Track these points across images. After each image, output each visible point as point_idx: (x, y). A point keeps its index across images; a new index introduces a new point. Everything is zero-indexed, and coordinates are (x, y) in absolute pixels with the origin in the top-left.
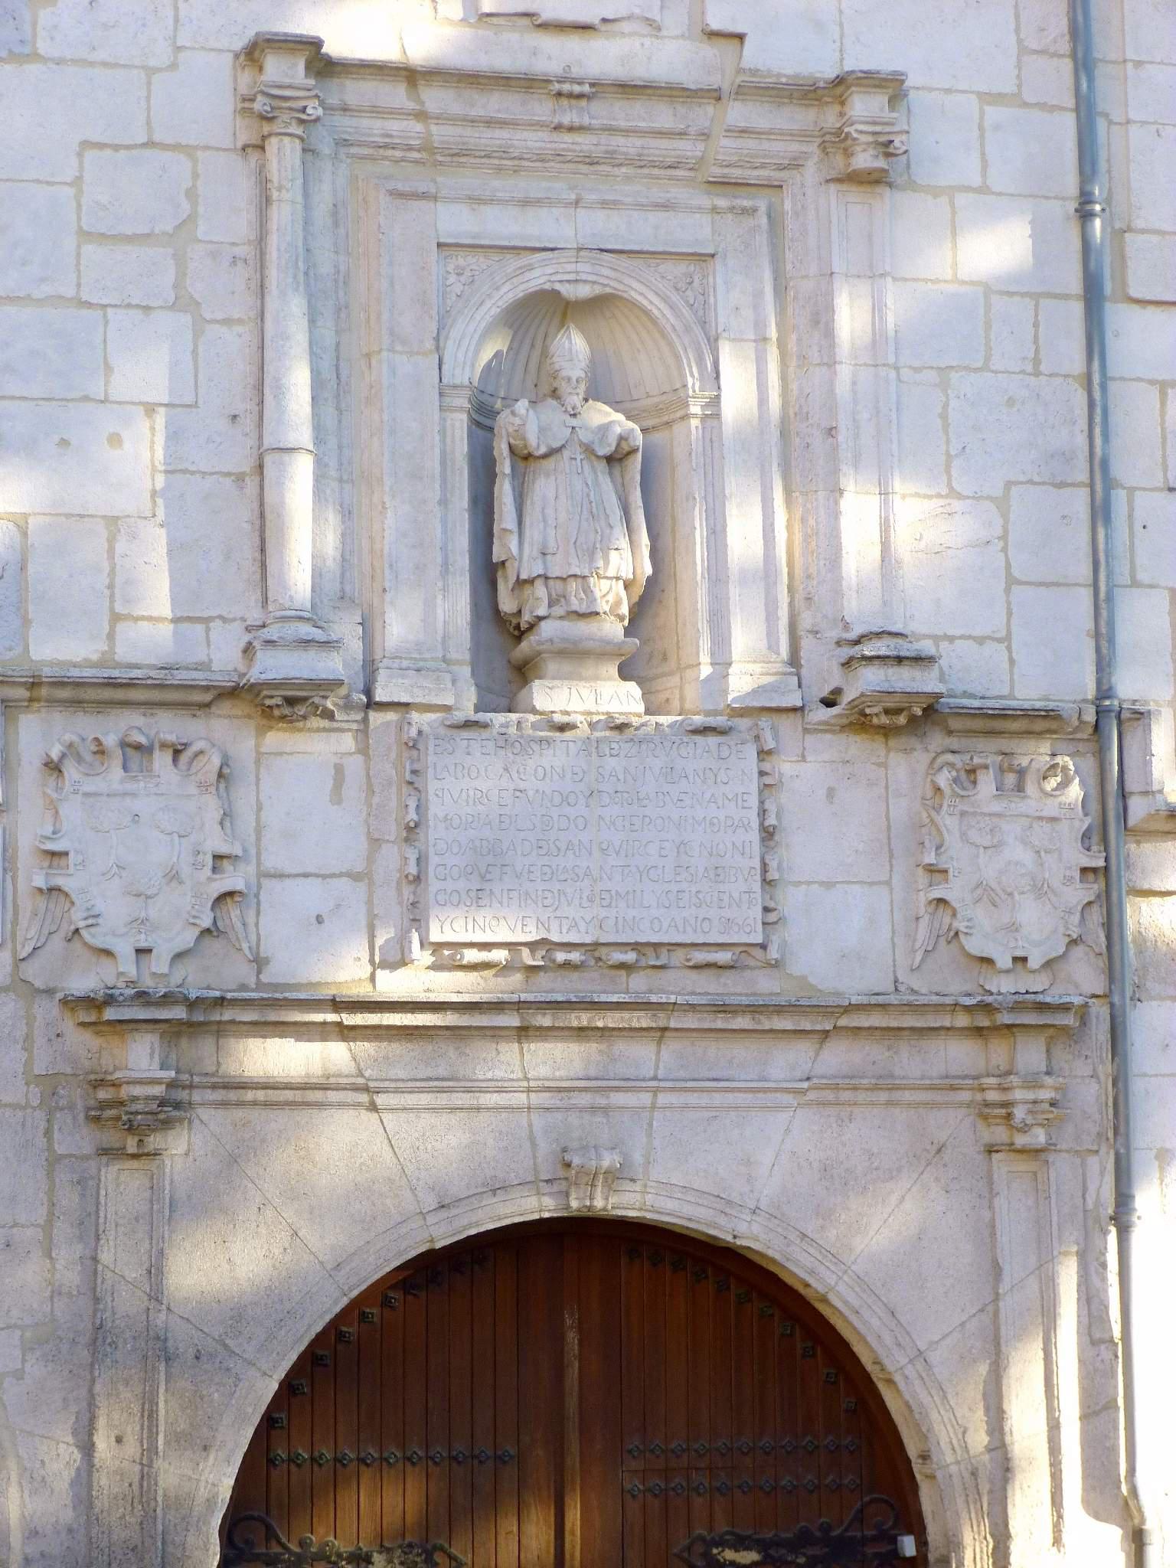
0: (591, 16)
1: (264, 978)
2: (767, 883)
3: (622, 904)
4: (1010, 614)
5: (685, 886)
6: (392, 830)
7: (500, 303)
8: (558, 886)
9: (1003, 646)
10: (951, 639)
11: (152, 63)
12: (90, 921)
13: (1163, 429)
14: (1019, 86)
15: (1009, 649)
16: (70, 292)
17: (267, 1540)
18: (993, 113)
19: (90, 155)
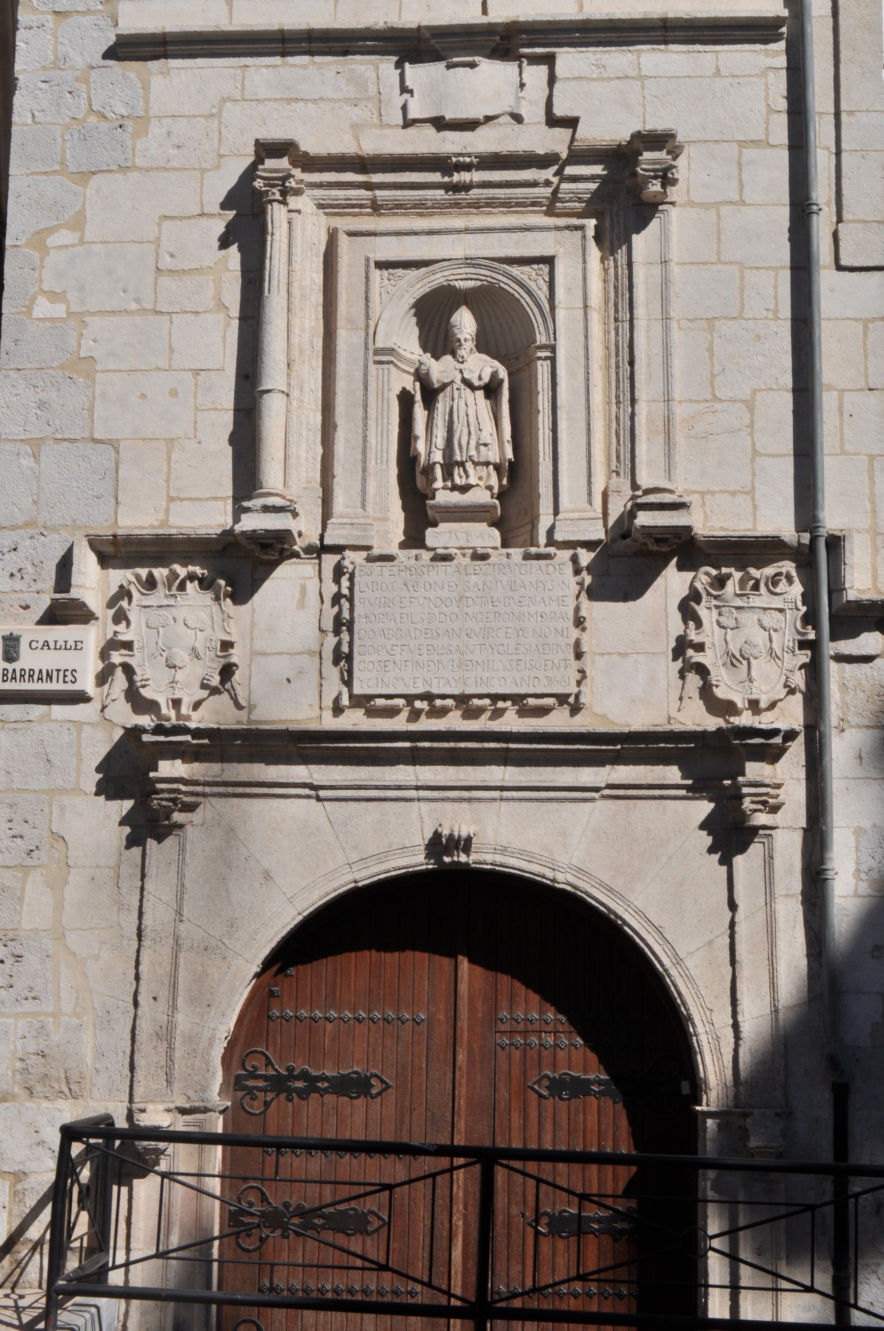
0: (479, 115)
1: (253, 717)
2: (579, 655)
3: (479, 669)
4: (754, 475)
5: (521, 657)
6: (329, 625)
7: (415, 296)
8: (437, 657)
9: (749, 497)
10: (712, 493)
11: (205, 165)
12: (144, 683)
13: (865, 350)
14: (767, 135)
15: (753, 499)
16: (149, 306)
17: (266, 1066)
18: (750, 154)
19: (167, 224)
